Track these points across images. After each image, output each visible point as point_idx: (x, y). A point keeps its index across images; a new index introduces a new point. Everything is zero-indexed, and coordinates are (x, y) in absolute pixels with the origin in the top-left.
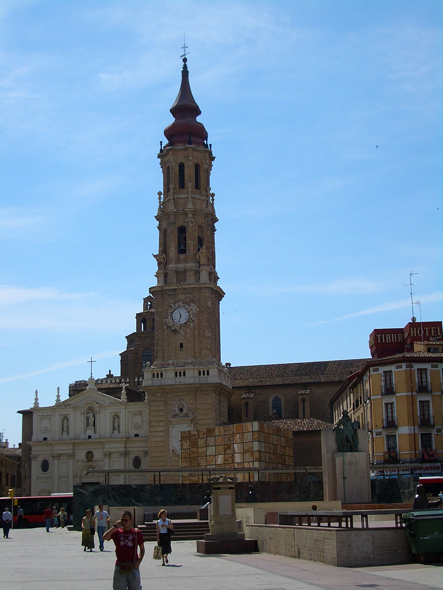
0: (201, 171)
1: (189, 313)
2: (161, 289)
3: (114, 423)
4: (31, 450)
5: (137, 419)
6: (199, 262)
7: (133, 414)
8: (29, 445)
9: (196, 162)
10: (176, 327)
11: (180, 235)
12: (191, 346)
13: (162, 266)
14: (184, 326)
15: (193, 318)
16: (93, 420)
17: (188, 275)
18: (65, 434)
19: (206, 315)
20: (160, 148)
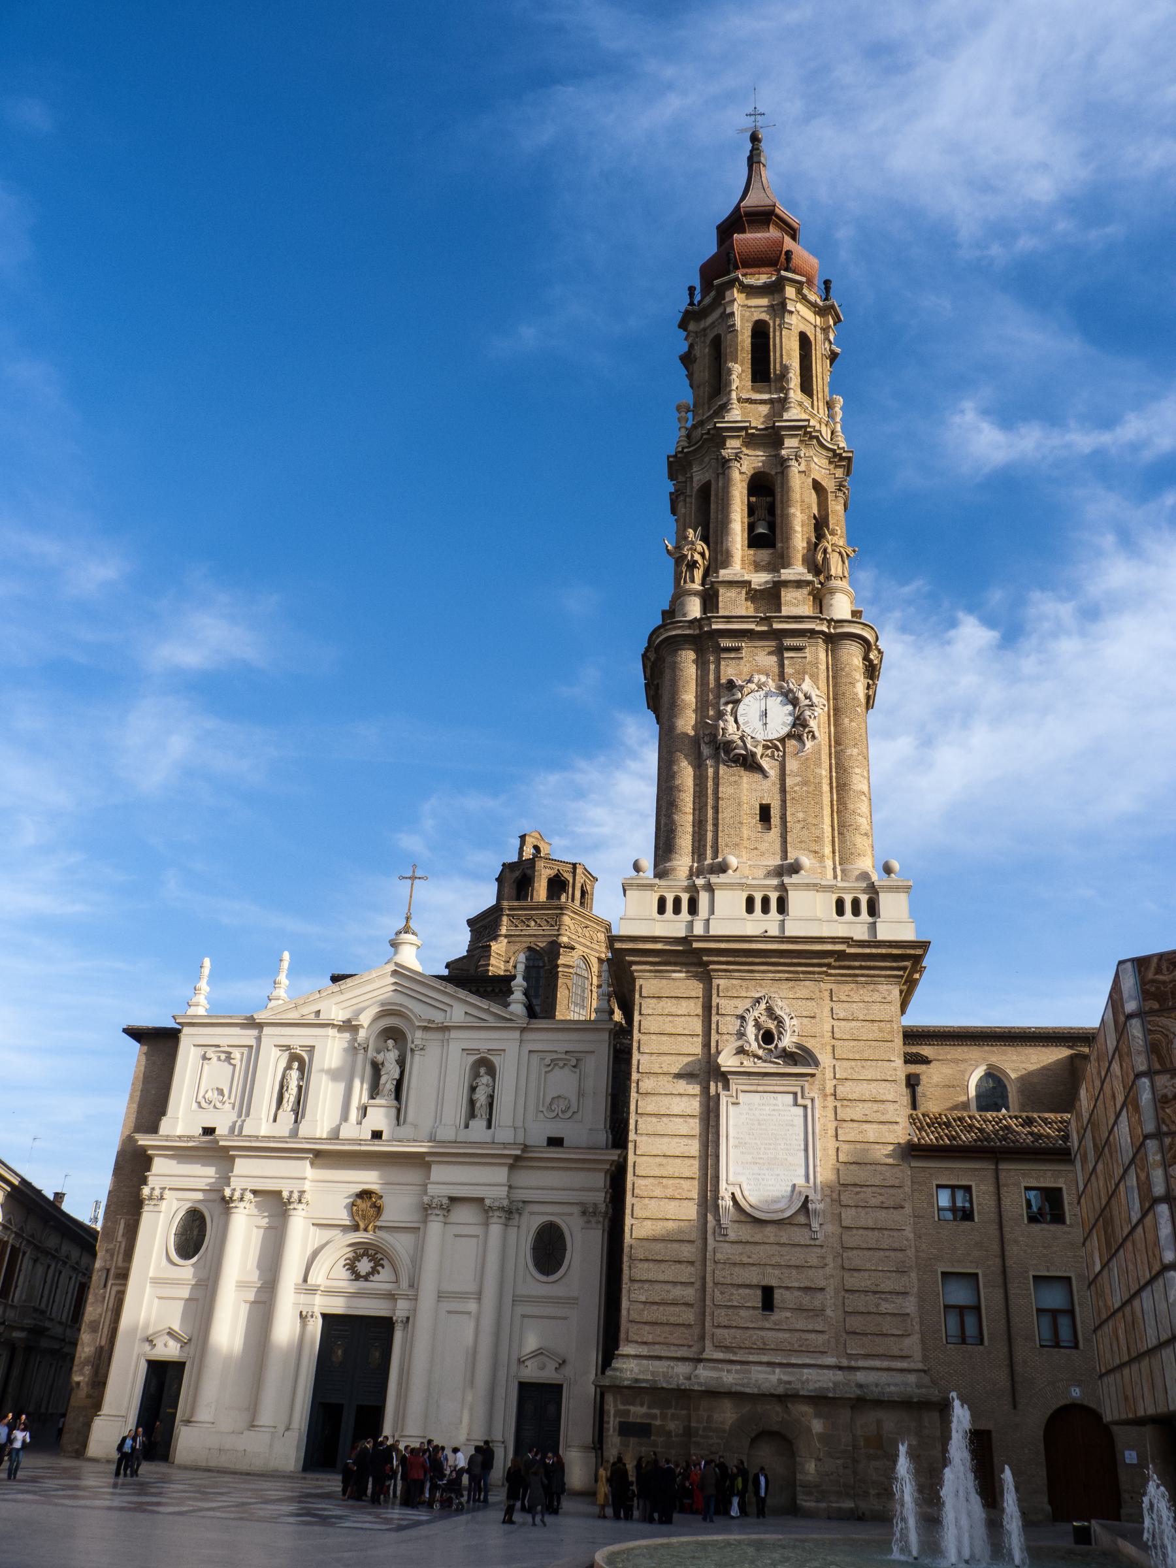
0: (814, 352)
1: (795, 707)
2: (697, 632)
3: (473, 1089)
4: (148, 1168)
5: (563, 1082)
6: (818, 568)
7: (547, 1061)
8: (144, 1149)
9: (803, 327)
10: (749, 746)
11: (753, 499)
12: (801, 815)
13: (698, 574)
14: (778, 750)
15: (813, 724)
16: (397, 1076)
17: (787, 598)
18: (287, 1116)
19: (851, 721)
20: (688, 301)
